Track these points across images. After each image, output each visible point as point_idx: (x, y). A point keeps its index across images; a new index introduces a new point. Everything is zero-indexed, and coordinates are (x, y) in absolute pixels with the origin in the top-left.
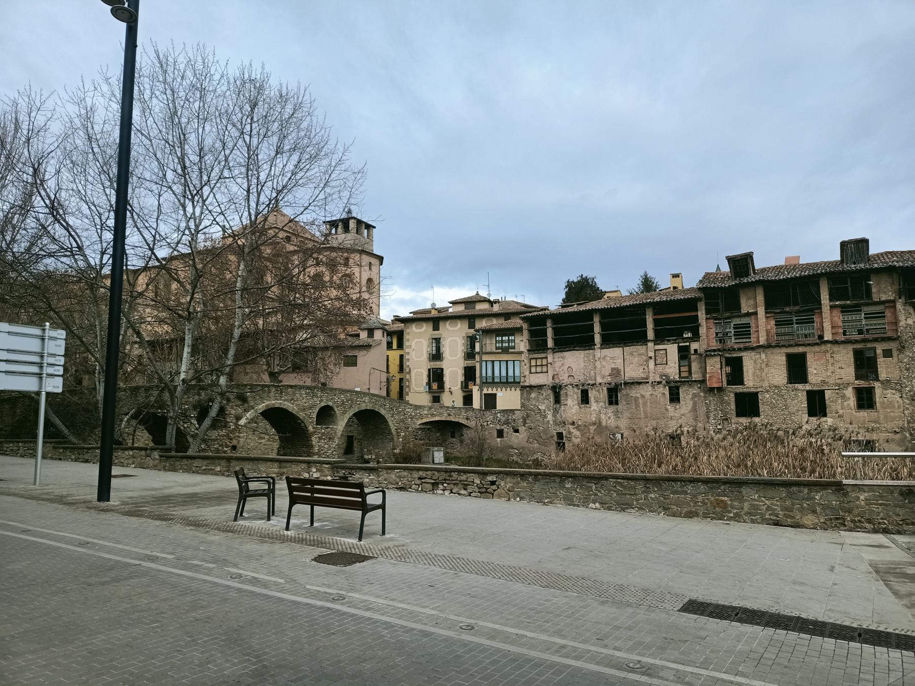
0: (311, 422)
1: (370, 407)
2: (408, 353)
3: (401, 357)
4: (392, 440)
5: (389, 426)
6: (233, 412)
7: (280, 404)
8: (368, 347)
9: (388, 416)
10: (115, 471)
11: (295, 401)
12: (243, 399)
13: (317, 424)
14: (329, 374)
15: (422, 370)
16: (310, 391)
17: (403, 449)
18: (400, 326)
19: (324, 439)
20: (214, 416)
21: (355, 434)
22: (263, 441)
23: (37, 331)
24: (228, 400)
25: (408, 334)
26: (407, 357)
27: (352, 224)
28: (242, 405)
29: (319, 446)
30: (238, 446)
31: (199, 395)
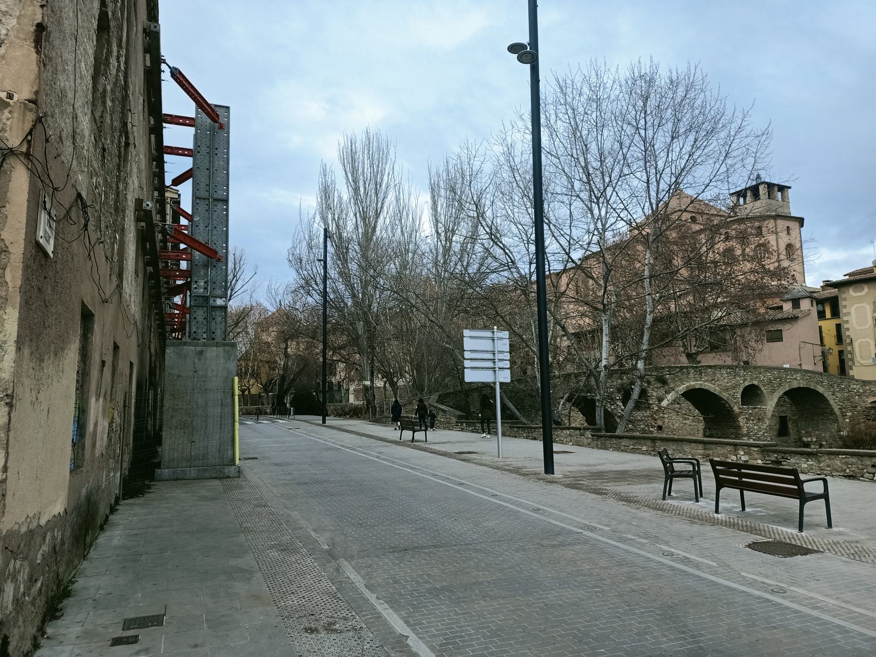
0: (735, 402)
1: (803, 384)
2: (847, 322)
3: (838, 327)
4: (836, 420)
5: (829, 405)
6: (655, 394)
7: (701, 385)
8: (795, 318)
9: (828, 395)
10: (556, 447)
11: (716, 381)
12: (663, 381)
13: (742, 405)
14: (751, 352)
15: (868, 340)
16: (731, 370)
17: (852, 430)
18: (834, 291)
19: (753, 420)
20: (636, 398)
21: (789, 414)
22: (688, 422)
23: (488, 334)
24: (649, 383)
25: (845, 299)
26: (846, 326)
27: (762, 190)
28: (663, 387)
29: (747, 427)
30: (664, 426)
31: (622, 379)
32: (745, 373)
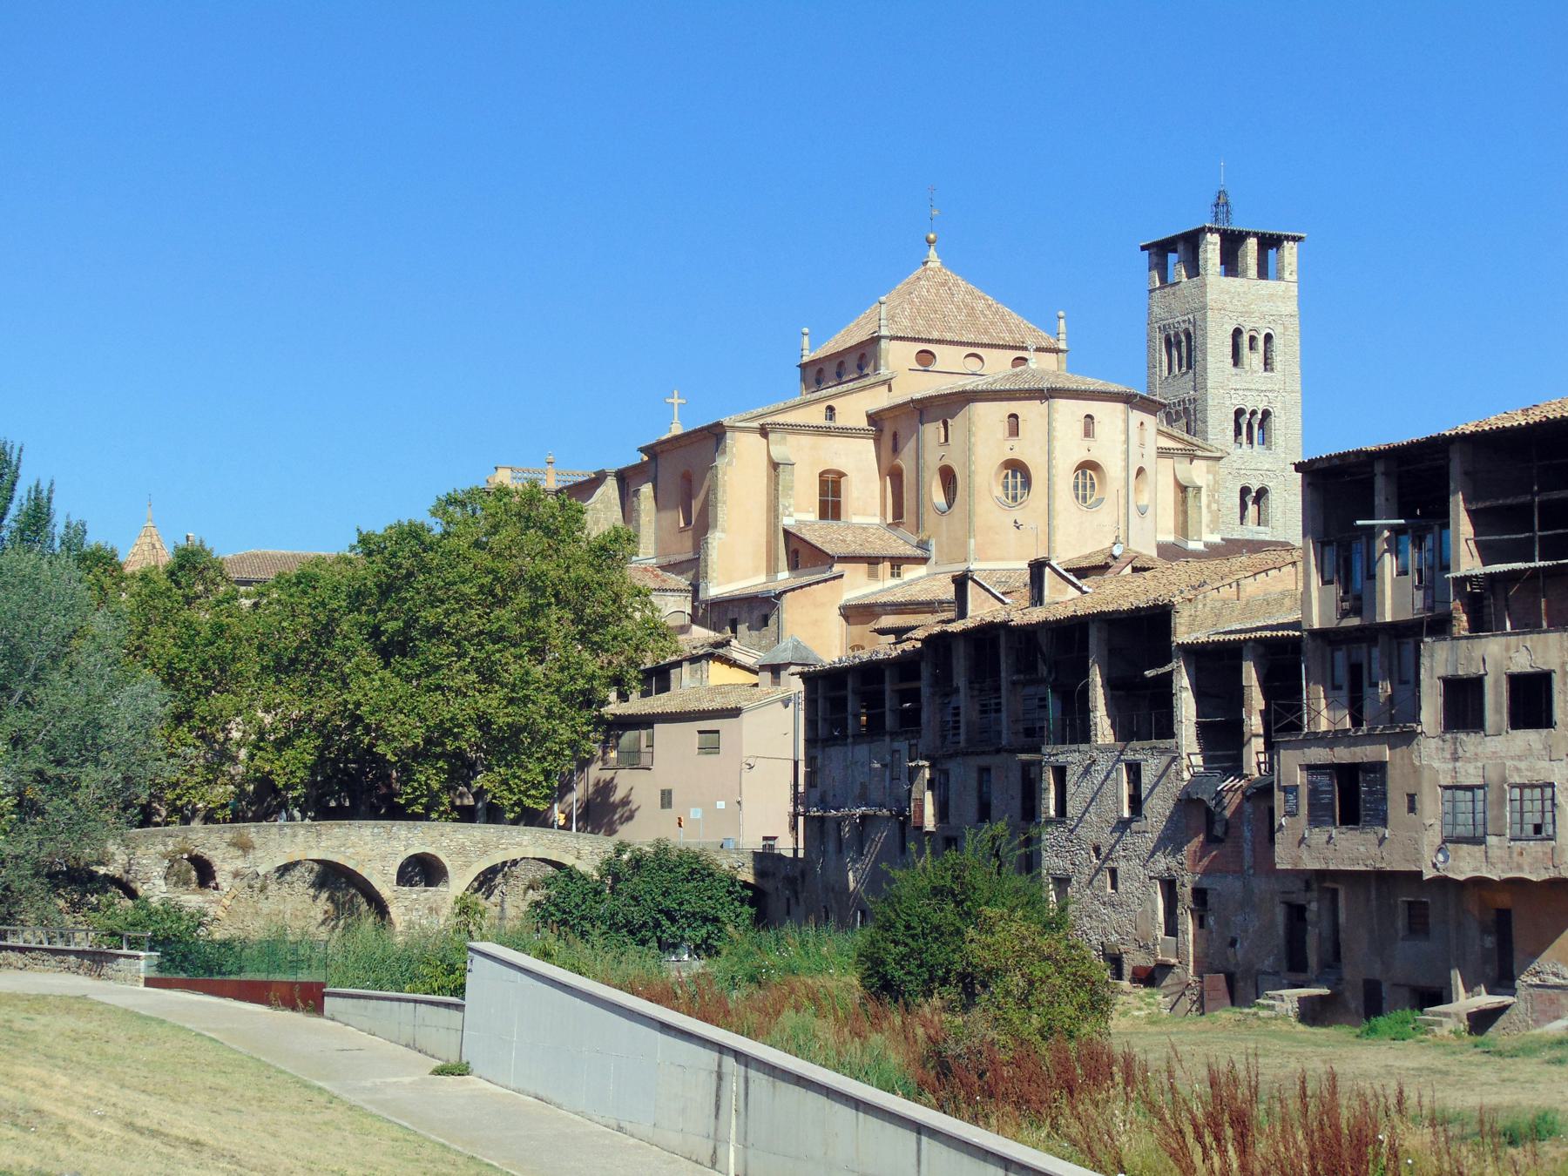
16: (382, 830)
32: (410, 835)
